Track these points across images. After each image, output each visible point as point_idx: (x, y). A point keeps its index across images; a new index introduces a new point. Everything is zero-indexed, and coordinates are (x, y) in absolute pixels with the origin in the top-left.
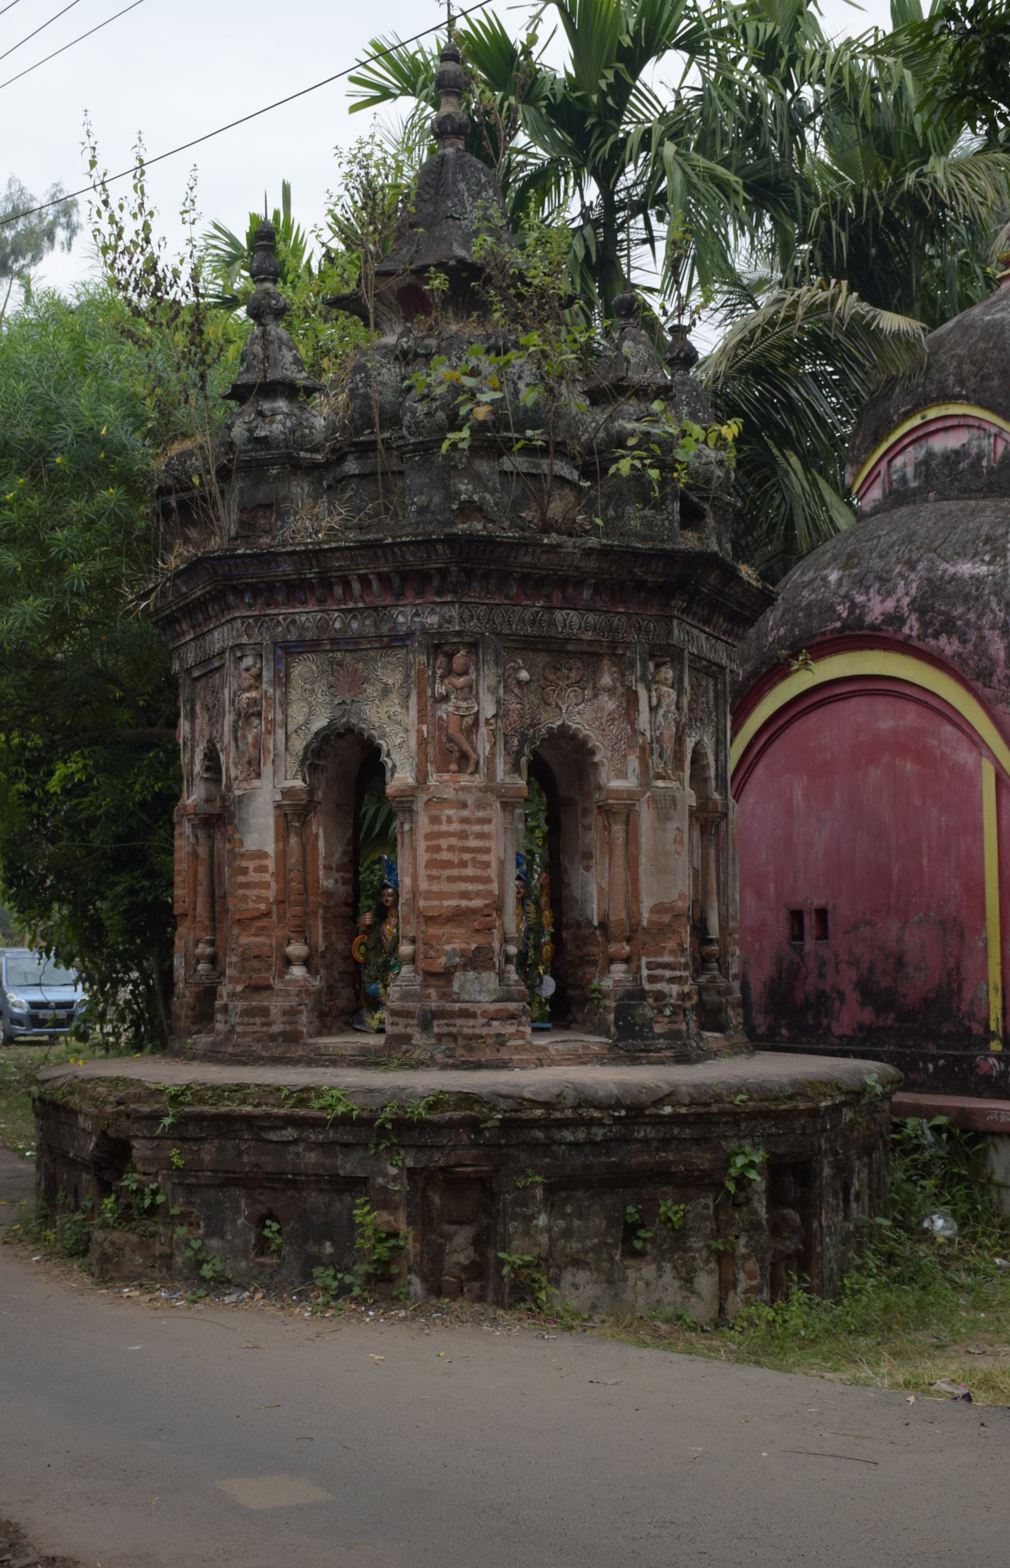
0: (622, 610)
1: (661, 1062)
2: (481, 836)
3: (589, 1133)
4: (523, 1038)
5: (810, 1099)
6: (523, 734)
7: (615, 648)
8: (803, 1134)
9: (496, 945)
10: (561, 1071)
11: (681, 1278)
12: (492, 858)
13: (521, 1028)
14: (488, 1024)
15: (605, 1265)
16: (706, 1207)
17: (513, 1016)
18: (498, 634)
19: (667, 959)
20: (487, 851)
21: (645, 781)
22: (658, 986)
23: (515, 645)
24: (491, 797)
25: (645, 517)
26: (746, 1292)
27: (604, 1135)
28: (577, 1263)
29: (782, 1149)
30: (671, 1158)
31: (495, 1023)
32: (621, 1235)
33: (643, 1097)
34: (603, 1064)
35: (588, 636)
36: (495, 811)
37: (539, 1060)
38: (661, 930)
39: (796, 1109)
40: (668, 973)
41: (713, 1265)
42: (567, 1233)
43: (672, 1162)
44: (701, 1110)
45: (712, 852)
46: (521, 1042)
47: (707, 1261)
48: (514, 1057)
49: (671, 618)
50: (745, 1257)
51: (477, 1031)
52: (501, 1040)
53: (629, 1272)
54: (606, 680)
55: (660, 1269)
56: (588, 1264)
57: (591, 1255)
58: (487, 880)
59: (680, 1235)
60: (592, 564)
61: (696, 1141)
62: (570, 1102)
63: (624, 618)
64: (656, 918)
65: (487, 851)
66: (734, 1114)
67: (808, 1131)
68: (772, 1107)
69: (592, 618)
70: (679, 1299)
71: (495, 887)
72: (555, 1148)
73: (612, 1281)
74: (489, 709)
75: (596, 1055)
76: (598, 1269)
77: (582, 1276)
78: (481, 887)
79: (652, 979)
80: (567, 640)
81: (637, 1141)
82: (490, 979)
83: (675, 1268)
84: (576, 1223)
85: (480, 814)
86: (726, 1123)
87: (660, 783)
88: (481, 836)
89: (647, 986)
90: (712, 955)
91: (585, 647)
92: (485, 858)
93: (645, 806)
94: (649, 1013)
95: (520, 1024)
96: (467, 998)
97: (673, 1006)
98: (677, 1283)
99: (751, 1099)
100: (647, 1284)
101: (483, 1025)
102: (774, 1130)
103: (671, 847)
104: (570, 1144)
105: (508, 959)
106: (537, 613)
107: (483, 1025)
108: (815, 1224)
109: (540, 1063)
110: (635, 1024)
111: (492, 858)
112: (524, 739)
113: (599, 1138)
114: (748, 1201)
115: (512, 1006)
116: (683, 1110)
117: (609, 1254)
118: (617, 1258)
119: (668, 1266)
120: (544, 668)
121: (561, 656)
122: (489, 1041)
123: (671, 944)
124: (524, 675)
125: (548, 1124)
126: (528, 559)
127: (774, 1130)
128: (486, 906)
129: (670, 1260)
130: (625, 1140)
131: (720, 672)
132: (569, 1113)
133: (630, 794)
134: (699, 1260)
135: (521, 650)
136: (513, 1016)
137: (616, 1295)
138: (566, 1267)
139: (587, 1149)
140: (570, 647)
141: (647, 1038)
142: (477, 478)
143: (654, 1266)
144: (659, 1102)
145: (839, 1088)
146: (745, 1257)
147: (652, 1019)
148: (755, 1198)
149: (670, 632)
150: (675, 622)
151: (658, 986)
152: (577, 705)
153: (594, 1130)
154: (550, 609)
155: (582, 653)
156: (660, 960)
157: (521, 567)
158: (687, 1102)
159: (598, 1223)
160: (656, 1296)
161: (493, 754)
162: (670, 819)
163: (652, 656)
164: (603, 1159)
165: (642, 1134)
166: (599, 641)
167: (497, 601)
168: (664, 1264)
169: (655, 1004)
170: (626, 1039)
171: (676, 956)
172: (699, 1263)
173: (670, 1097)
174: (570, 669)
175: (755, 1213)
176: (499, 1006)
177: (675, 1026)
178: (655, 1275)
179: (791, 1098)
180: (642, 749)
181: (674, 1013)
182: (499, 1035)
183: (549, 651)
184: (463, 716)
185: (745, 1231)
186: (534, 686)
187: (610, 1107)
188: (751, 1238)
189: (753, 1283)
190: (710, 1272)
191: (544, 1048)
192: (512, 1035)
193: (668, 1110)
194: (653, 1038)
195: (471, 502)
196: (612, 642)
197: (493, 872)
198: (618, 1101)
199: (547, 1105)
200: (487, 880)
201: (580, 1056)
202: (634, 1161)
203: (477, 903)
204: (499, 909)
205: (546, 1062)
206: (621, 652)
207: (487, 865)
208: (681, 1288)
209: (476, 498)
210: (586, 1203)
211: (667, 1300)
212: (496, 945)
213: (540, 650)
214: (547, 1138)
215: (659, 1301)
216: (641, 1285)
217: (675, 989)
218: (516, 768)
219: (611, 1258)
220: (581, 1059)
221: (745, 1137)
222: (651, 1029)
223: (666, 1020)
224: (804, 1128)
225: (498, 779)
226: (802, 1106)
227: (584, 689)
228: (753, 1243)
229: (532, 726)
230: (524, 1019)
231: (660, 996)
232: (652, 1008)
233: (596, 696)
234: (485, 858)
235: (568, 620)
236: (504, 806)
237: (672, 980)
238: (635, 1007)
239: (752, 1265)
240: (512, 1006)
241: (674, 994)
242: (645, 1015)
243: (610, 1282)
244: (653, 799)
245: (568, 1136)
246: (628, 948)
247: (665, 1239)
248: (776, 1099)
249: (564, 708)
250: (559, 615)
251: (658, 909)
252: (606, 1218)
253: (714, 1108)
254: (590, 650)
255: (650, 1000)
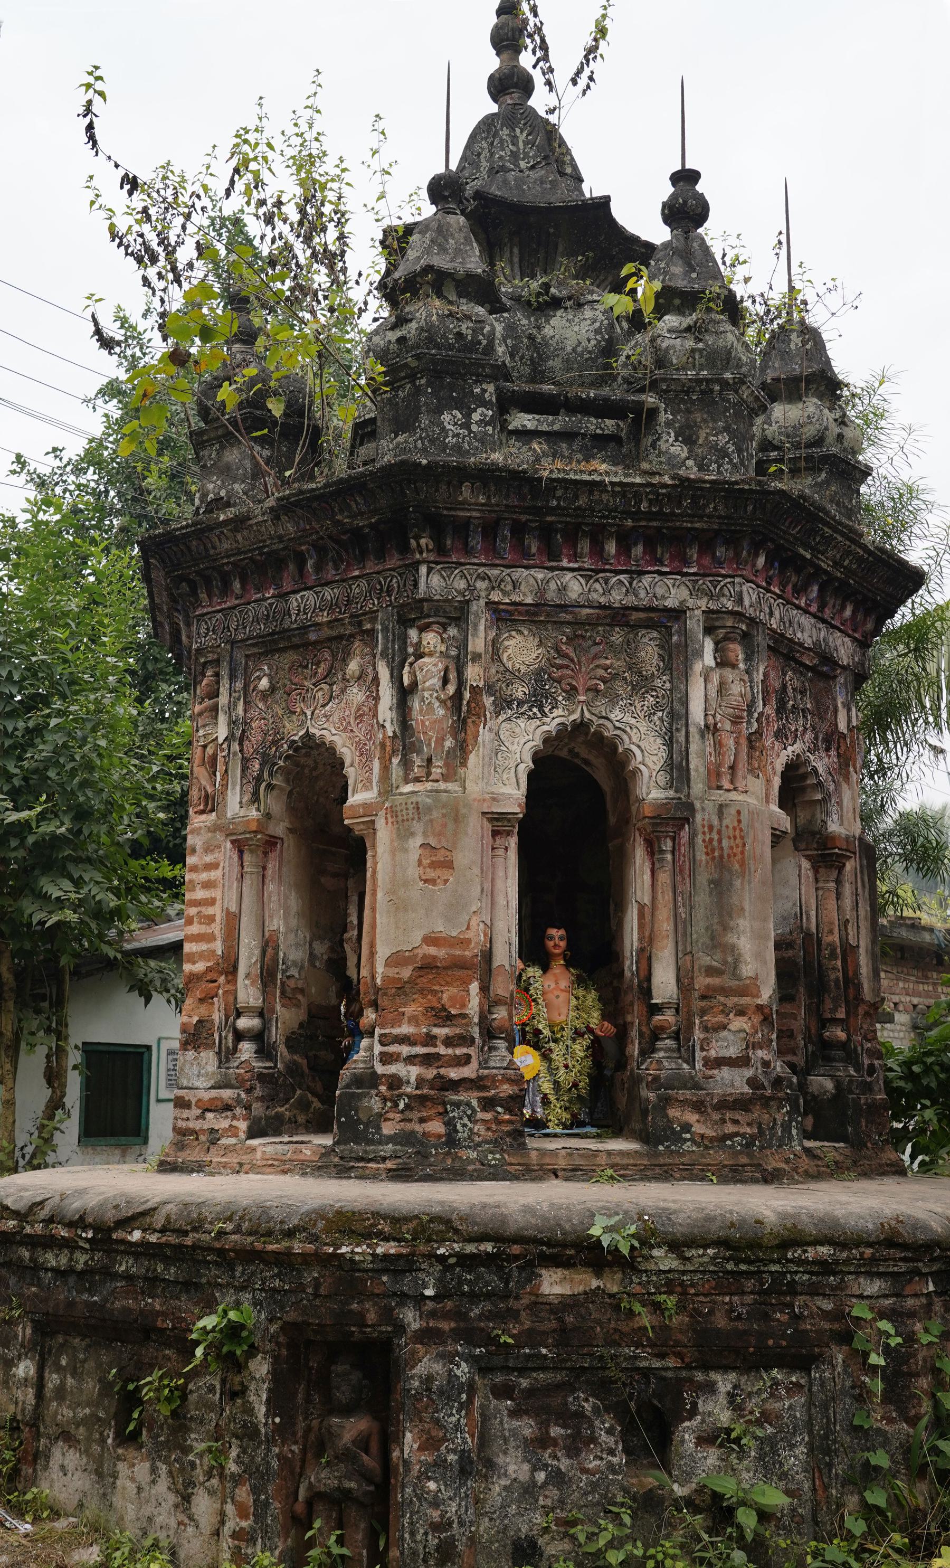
0: (357, 573)
1: (374, 1177)
2: (208, 885)
3: (71, 1259)
4: (236, 1136)
5: (313, 1238)
6: (264, 755)
7: (360, 624)
8: (316, 1295)
9: (217, 1017)
10: (601, 1196)
11: (177, 1492)
12: (216, 911)
13: (235, 1123)
14: (202, 1117)
15: (96, 1448)
16: (211, 1389)
17: (228, 1108)
18: (233, 643)
19: (405, 1029)
20: (211, 902)
21: (387, 789)
22: (392, 1069)
23: (256, 650)
24: (220, 836)
25: (398, 444)
26: (235, 1535)
27: (86, 1263)
28: (66, 1437)
29: (292, 1316)
30: (158, 1307)
31: (210, 1115)
32: (113, 1410)
33: (110, 1216)
34: (304, 1174)
35: (324, 618)
36: (226, 853)
37: (241, 1164)
38: (401, 989)
39: (288, 1253)
40: (405, 1050)
41: (215, 1482)
42: (60, 1393)
43: (158, 1313)
44: (172, 1239)
45: (664, 877)
46: (233, 1141)
47: (209, 1475)
48: (215, 1160)
49: (416, 565)
50: (237, 1480)
51: (191, 1125)
52: (214, 1136)
53: (122, 1467)
54: (353, 666)
55: (154, 1470)
56: (79, 1442)
57: (82, 1429)
58: (210, 938)
59: (180, 1422)
60: (289, 528)
61: (187, 1286)
62: (44, 1213)
63: (363, 583)
64: (392, 972)
65: (211, 902)
66: (221, 1252)
67: (322, 1291)
68: (259, 1246)
69: (328, 593)
70: (173, 1524)
71: (218, 947)
72: (42, 1274)
73: (103, 1475)
74: (222, 732)
75: (302, 1162)
76: (87, 1452)
77: (72, 1458)
78: (204, 946)
79: (387, 1059)
80: (304, 629)
81: (116, 1276)
82: (209, 1059)
83: (170, 1473)
84: (70, 1381)
85: (208, 859)
86: (216, 1263)
87: (408, 788)
88: (208, 885)
89: (380, 1069)
90: (662, 1029)
91: (327, 632)
92: (210, 911)
93: (383, 821)
94: (375, 1104)
95: (234, 1117)
96: (185, 1083)
97: (409, 1097)
98: (172, 1498)
99: (238, 1230)
100: (139, 1489)
101: (197, 1118)
102: (277, 1283)
103: (413, 872)
104: (53, 1269)
105: (239, 1036)
106: (271, 605)
107: (197, 1118)
108: (396, 1454)
109: (238, 1170)
110: (359, 1121)
111: (216, 911)
112: (266, 761)
113: (80, 1267)
114: (242, 1392)
115: (227, 1094)
116: (153, 1238)
117: (101, 1434)
118: (110, 1441)
119: (163, 1468)
120: (290, 669)
121: (310, 651)
122: (203, 1138)
123: (409, 1010)
124: (264, 683)
125: (34, 1242)
126: (226, 546)
127: (277, 1283)
128: (209, 969)
129: (166, 1461)
130: (108, 1273)
131: (677, 619)
132: (39, 1228)
133: (369, 809)
134: (199, 1470)
135: (265, 654)
136: (228, 1108)
137: (104, 1495)
138: (57, 1439)
139: (72, 1280)
140: (313, 637)
141: (370, 1142)
142: (226, 472)
143: (148, 1465)
144: (127, 1222)
145: (456, 1231)
146: (237, 1480)
147: (380, 1115)
148: (252, 1387)
149: (416, 584)
150: (423, 569)
151: (392, 1069)
152: (323, 706)
153: (77, 1255)
154: (283, 596)
155: (330, 639)
156: (396, 1031)
157: (228, 557)
158: (159, 1226)
159: (91, 1386)
160: (147, 1510)
161: (225, 786)
162: (412, 834)
163: (405, 623)
164: (85, 1296)
165: (123, 1268)
166: (337, 620)
167: (229, 604)
168: (159, 1464)
169: (388, 1094)
170: (346, 1142)
171: (417, 1025)
172: (199, 1474)
173: (140, 1217)
174: (318, 664)
175: (249, 1410)
176: (214, 1093)
177: (408, 1126)
178: (148, 1478)
179: (290, 1234)
180: (383, 745)
181: (407, 1106)
182: (212, 1131)
183: (295, 647)
184: (205, 747)
185: (237, 1437)
186: (278, 695)
187: (71, 1225)
188: (244, 1451)
189: (244, 1524)
190: (211, 1492)
191: (254, 1150)
192: (225, 1130)
193: (137, 1235)
194: (380, 1143)
195: (218, 499)
196: (352, 616)
197: (217, 928)
198: (82, 1218)
199: (16, 1214)
200: (210, 938)
201: (284, 1162)
202: (117, 1304)
203: (200, 967)
204: (232, 971)
205: (246, 1167)
206: (368, 626)
207: (211, 919)
208: (176, 1506)
209: (223, 493)
210: (81, 1356)
211: (159, 1520)
212: (217, 1017)
213: (284, 650)
214: (31, 1259)
215: (150, 1519)
216: (131, 1487)
217: (414, 1072)
218: (255, 798)
219: (103, 1441)
220: (283, 1167)
221: (243, 1288)
222: (379, 1128)
223: (398, 1117)
224: (317, 1284)
225: (229, 815)
226: (297, 1248)
227: (331, 685)
228: (246, 1460)
229: (275, 743)
230: (238, 1111)
231: (395, 1082)
232: (385, 1100)
233: (343, 691)
234: (210, 911)
235: (304, 603)
236: (240, 847)
237: (411, 1060)
238: (359, 1097)
239: (243, 1493)
240: (227, 1094)
241: (413, 1079)
242: (371, 1109)
243: (99, 1474)
244: (393, 811)
245: (51, 1259)
246: (373, 1016)
247: (161, 1427)
248: (269, 1233)
249: (309, 713)
250: (294, 602)
251: (396, 960)
252: (100, 1381)
253: (188, 1241)
254: (334, 633)
255: (383, 1088)
